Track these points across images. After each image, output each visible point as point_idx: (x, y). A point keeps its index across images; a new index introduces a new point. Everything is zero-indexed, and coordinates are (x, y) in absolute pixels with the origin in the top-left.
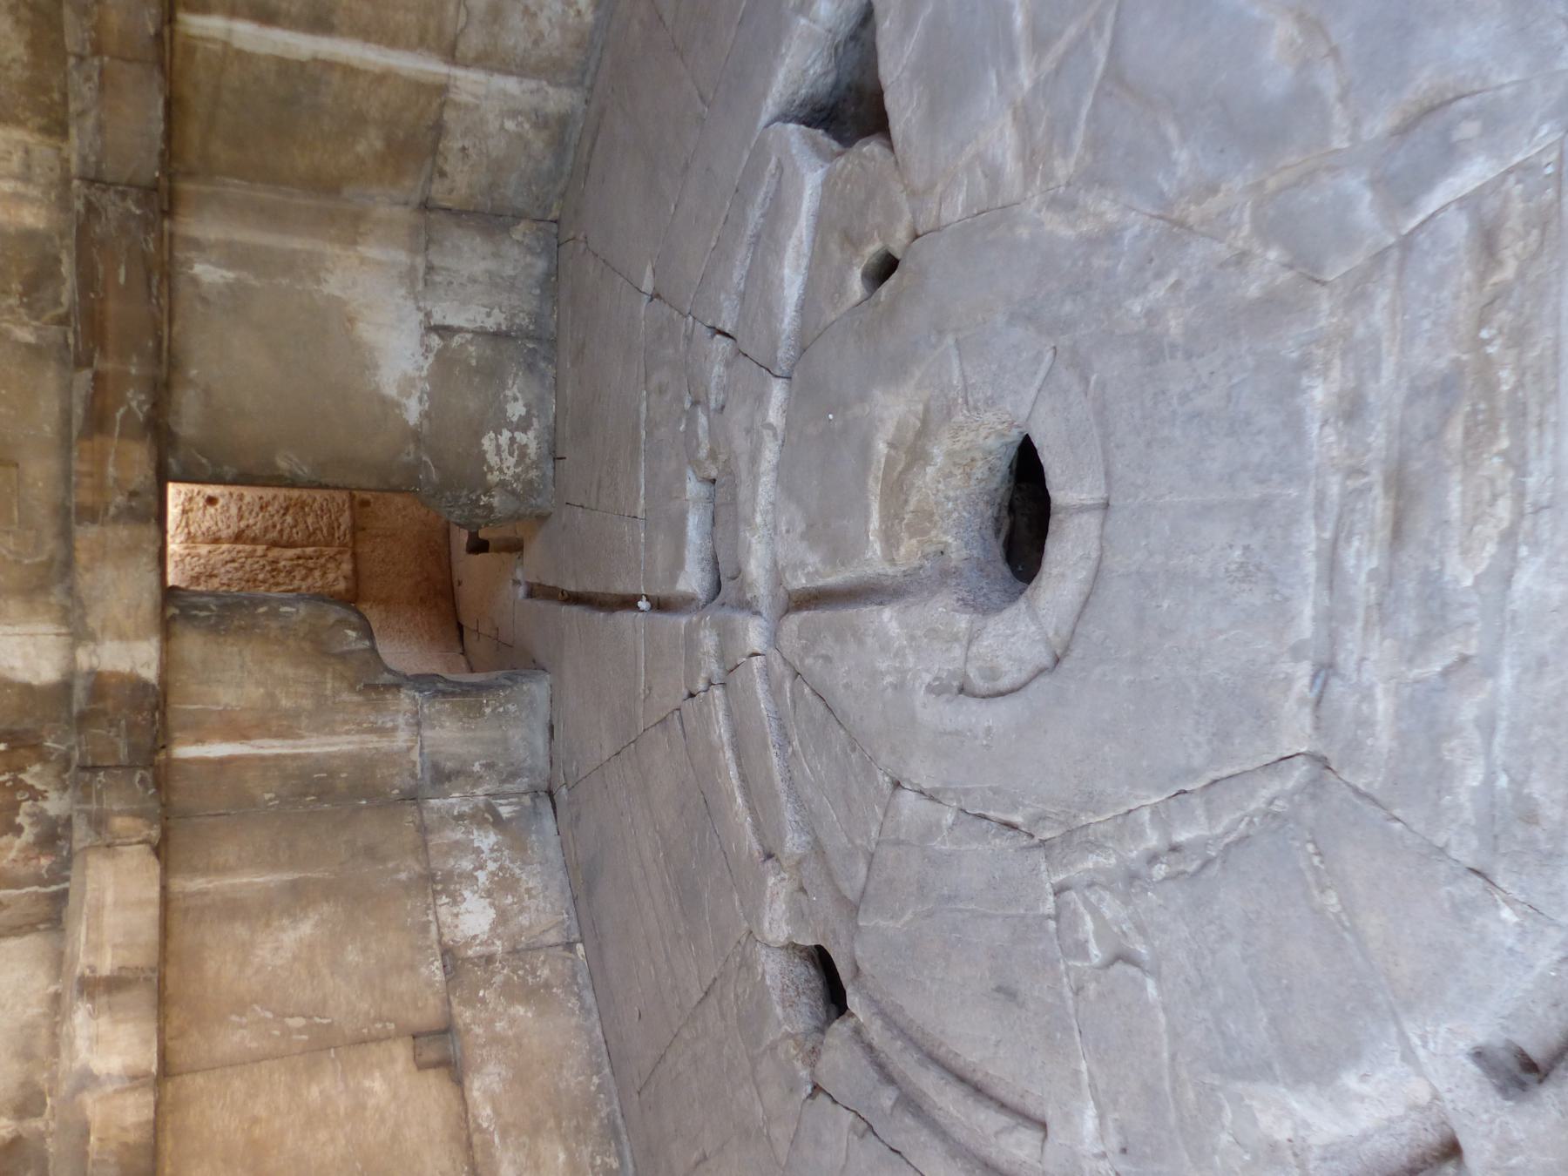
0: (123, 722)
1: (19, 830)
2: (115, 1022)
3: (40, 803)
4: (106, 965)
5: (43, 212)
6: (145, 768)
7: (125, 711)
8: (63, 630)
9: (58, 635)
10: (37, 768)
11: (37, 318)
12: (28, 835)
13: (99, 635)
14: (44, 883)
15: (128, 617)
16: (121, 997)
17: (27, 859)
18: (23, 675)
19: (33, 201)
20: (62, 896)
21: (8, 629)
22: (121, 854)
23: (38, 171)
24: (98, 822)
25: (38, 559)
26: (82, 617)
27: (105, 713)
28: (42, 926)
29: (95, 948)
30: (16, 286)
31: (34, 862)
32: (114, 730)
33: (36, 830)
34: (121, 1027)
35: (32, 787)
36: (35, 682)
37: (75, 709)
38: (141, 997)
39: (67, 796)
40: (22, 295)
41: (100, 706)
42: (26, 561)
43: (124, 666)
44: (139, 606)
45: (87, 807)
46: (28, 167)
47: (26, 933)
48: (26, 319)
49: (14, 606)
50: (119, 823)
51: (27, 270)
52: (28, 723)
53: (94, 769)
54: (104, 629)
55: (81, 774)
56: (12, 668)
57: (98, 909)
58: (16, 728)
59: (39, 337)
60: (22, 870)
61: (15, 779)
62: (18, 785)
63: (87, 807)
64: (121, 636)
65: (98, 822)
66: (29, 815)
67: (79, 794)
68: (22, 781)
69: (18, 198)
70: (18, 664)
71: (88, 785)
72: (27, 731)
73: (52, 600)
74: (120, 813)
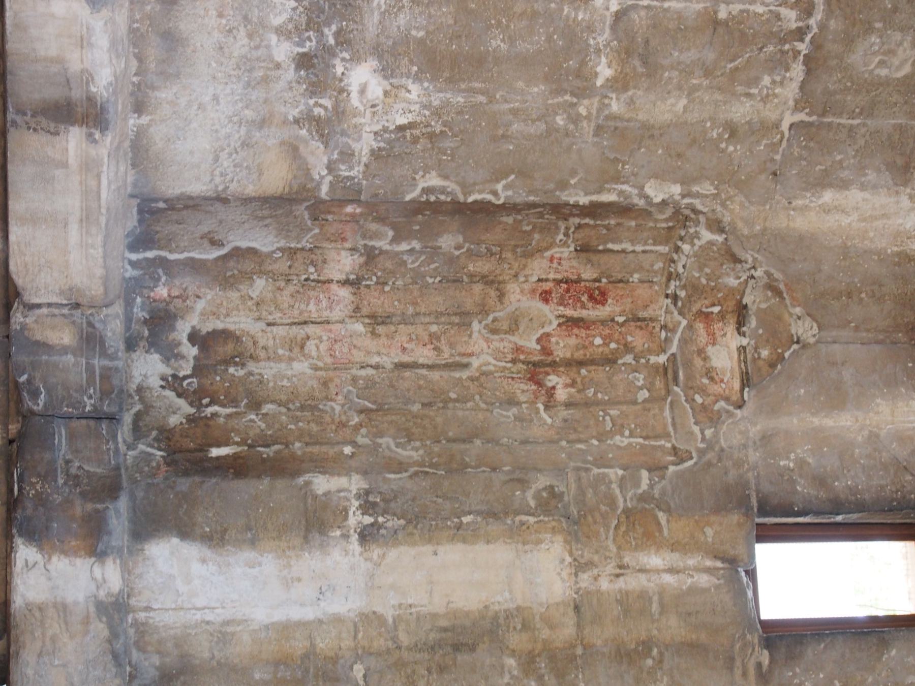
0: (61, 481)
1: (194, 337)
2: (59, 60)
3: (169, 371)
4: (74, 140)
6: (33, 413)
7: (58, 499)
8: (142, 616)
9: (148, 609)
10: (174, 420)
12: (183, 329)
13: (92, 609)
14: (162, 262)
15: (54, 639)
16: (52, 93)
17: (183, 297)
18: (191, 551)
20: (142, 240)
21: (209, 617)
22: (62, 293)
24: (91, 340)
26: (114, 635)
27: (83, 495)
28: (161, 205)
29: (89, 166)
31: (175, 293)
32: (73, 471)
33: (173, 336)
34: (53, 52)
35: (179, 395)
36: (175, 541)
37: (123, 502)
38: (27, 87)
39: (138, 380)
41: (90, 506)
43: (59, 563)
44: (40, 655)
45: (106, 363)
47: (179, 198)
49: (202, 650)
50: (65, 337)
52: (184, 484)
53: (98, 417)
54: (86, 621)
55: (114, 409)
56: (204, 561)
57: (87, 219)
58: (197, 479)
60: (189, 282)
61: (200, 407)
62: (196, 397)
63: (106, 363)
64: (63, 609)
65: (91, 340)
66: (180, 356)
67: (115, 382)
68: (191, 404)
70: (196, 568)
71: (105, 394)
72: (186, 473)
73: (156, 660)
74: (65, 350)
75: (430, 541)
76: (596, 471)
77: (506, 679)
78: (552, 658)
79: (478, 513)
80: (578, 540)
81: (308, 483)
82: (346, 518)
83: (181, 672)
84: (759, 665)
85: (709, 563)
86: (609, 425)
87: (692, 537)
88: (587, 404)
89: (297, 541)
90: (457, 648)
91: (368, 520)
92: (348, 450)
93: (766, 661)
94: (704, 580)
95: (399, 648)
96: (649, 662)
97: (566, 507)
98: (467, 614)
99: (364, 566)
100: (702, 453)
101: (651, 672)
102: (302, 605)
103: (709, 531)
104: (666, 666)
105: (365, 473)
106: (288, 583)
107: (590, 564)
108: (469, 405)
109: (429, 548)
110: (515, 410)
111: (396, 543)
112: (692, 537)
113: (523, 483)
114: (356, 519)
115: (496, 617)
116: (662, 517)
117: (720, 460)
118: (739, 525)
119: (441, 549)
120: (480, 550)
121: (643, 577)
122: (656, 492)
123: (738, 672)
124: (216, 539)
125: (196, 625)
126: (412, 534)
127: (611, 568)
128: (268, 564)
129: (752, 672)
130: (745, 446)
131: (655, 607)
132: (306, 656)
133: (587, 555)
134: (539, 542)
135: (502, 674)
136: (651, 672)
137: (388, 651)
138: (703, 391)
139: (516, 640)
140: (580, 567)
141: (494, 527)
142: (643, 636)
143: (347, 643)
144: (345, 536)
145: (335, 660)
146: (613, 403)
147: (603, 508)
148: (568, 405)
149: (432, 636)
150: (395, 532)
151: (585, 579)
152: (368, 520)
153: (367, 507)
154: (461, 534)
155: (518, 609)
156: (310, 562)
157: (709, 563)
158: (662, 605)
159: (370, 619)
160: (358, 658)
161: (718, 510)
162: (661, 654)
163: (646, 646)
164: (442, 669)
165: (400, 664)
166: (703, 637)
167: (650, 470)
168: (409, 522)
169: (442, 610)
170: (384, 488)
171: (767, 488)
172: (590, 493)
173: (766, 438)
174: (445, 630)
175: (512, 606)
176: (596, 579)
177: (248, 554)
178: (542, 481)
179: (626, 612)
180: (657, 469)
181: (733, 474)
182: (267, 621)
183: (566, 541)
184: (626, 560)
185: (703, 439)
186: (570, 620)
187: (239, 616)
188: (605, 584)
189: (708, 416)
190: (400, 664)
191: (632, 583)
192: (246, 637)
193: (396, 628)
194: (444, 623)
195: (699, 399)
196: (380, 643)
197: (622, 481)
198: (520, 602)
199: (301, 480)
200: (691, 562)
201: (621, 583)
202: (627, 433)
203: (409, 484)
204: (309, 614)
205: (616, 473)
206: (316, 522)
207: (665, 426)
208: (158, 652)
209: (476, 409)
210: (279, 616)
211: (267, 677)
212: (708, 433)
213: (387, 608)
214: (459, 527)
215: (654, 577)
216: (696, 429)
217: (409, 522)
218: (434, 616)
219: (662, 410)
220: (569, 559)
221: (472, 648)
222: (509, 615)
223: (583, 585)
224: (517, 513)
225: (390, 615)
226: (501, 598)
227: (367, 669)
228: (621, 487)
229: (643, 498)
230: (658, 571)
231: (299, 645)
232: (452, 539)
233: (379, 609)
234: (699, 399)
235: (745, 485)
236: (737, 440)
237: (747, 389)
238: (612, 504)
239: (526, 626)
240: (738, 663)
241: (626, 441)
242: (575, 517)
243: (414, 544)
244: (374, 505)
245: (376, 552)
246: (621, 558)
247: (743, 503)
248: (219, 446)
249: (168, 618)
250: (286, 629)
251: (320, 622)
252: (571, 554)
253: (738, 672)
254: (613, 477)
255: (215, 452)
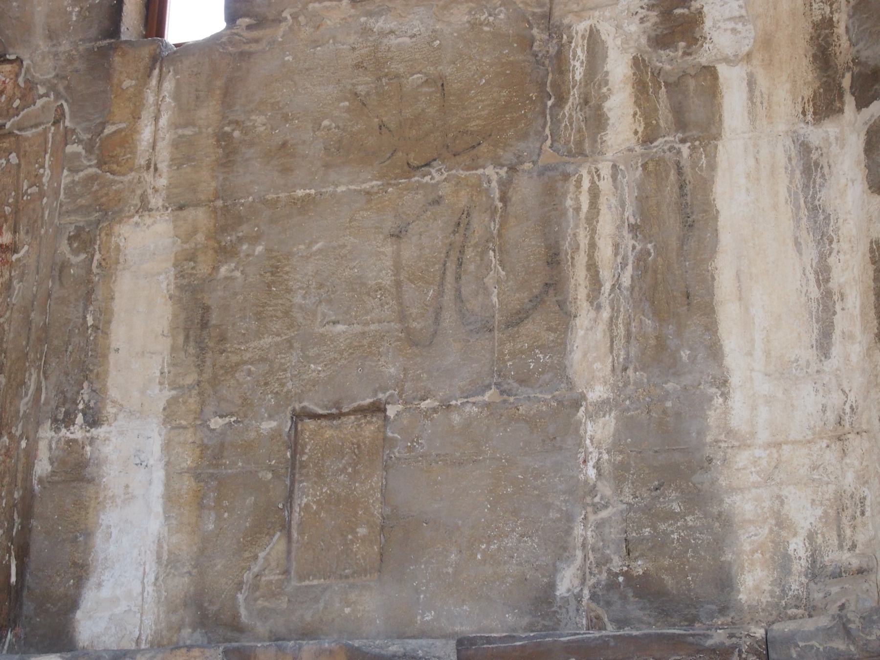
5: (765, 599)
11: (594, 597)
18: (90, 598)
19: (781, 583)
21: (151, 578)
23: (835, 589)
25: (243, 612)
30: (639, 567)
36: (79, 615)
40: (625, 574)
42: (240, 597)
46: (838, 574)
48: (592, 581)
49: (181, 584)
51: (669, 581)
52: (29, 607)
56: (99, 585)
59: (566, 600)
69: (782, 563)
70: (105, 592)
75: (105, 356)
76: (62, 196)
77: (238, 274)
78: (223, 229)
79: (86, 308)
80: (121, 211)
81: (40, 481)
82: (75, 441)
83: (200, 607)
84: (249, 27)
85: (154, 82)
86: (35, 189)
87: (129, 99)
88: (16, 212)
89: (91, 489)
90: (204, 324)
91: (80, 419)
92: (23, 444)
93: (247, 21)
94: (169, 86)
95: (199, 383)
96: (236, 134)
97: (89, 224)
98: (175, 316)
99: (121, 421)
100: (58, 96)
101: (245, 132)
102: (150, 483)
103: (127, 83)
104: (242, 117)
105: (38, 424)
106: (129, 497)
107: (144, 199)
108: (6, 328)
109: (112, 358)
110: (15, 282)
111: (104, 389)
112: (129, 99)
113: (64, 266)
114: (77, 432)
115: (180, 288)
116: (109, 130)
117: (64, 78)
118: (124, 55)
119: (114, 345)
120: (118, 305)
121: (160, 145)
122: (86, 137)
123: (254, 47)
124: (81, 572)
125: (158, 591)
126: (98, 374)
127: (148, 177)
128: (110, 518)
129: (255, 34)
130: (56, 55)
131: (188, 132)
132: (198, 477)
133: (136, 201)
134: (118, 248)
135: (235, 278)
136: (245, 132)
137: (200, 394)
138: (10, 100)
139: (203, 269)
140: (144, 207)
141: (100, 293)
142: (212, 141)
143: (189, 436)
144: (92, 441)
145: (203, 447)
146: (17, 187)
147: (95, 187)
148: (15, 231)
149: (191, 350)
150: (94, 391)
151: (156, 201)
152: (80, 419)
153: (68, 420)
154: (102, 328)
155: (175, 266)
156: (112, 477)
157: (154, 82)
158: (185, 126)
159: (169, 414)
160: (205, 424)
161: (108, 76)
162: (230, 123)
163: (222, 138)
164: (223, 339)
165: (214, 381)
166: (219, 83)
167: (66, 144)
168: (86, 378)
169: (169, 341)
170: (53, 404)
171: (94, 32)
172: (82, 201)
173: (52, 35)
174: (187, 337)
175: (172, 272)
176: (156, 190)
177: (98, 539)
178: (64, 247)
179: (188, 159)
180: (67, 137)
181: (79, 65)
182: (161, 518)
183: (120, 222)
184: (143, 162)
185: (47, 95)
186: (191, 214)
187: (154, 547)
188: (163, 182)
189: (28, 93)
190: (214, 381)
191: (164, 155)
192: (174, 540)
193: (181, 387)
194: (181, 339)
195: (17, 103)
196: (193, 402)
197: (74, 171)
198: (169, 264)
199: (37, 488)
200: (151, 99)
201: (163, 166)
202: (41, 171)
203: (53, 379)
204: (159, 475)
205: (66, 178)
206: (76, 470)
207: (40, 134)
208: (179, 629)
209: (9, 321)
210: (158, 507)
211: (213, 517)
212: (42, 90)
213: (161, 396)
214: (96, 327)
215: (161, 134)
216: (40, 103)
217: (86, 378)
218: (174, 349)
219: (26, 139)
220: (136, 218)
221: (207, 309)
222: (180, 274)
223: (160, 203)
224: (89, 271)
225: (168, 394)
226: (165, 282)
227: (216, 414)
228: (77, 171)
229: (89, 149)
230: (156, 131)
231: (187, 484)
232: (106, 334)
233: (162, 404)
234: (17, 103)
235: (90, 51)
236: (49, 63)
237: (8, 56)
238: (92, 178)
239: (192, 257)
240: (246, 48)
241: (48, 172)
242: (101, 212)
243: (107, 372)
244: (67, 414)
245: (110, 410)
246: (140, 167)
247: (104, 54)
248: (10, 576)
249: (149, 620)
250: (170, 499)
251: (168, 464)
252: (132, 216)
253: (254, 47)
254: (69, 180)
255: (13, 579)
